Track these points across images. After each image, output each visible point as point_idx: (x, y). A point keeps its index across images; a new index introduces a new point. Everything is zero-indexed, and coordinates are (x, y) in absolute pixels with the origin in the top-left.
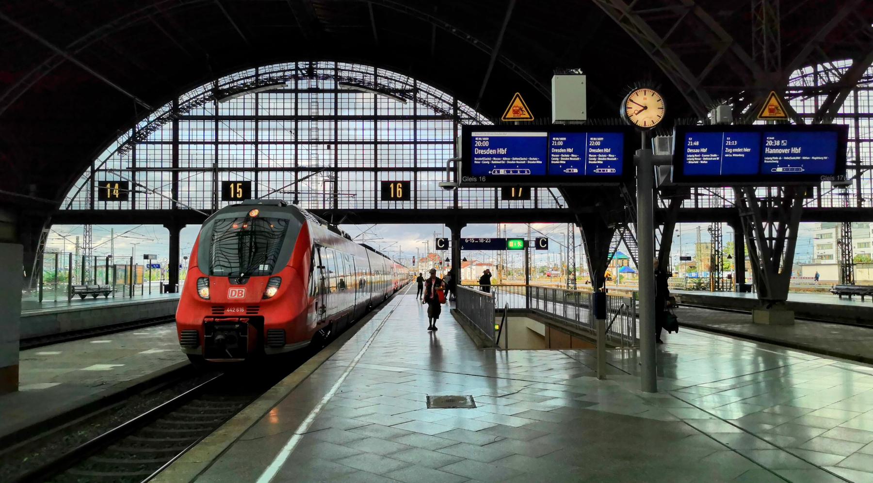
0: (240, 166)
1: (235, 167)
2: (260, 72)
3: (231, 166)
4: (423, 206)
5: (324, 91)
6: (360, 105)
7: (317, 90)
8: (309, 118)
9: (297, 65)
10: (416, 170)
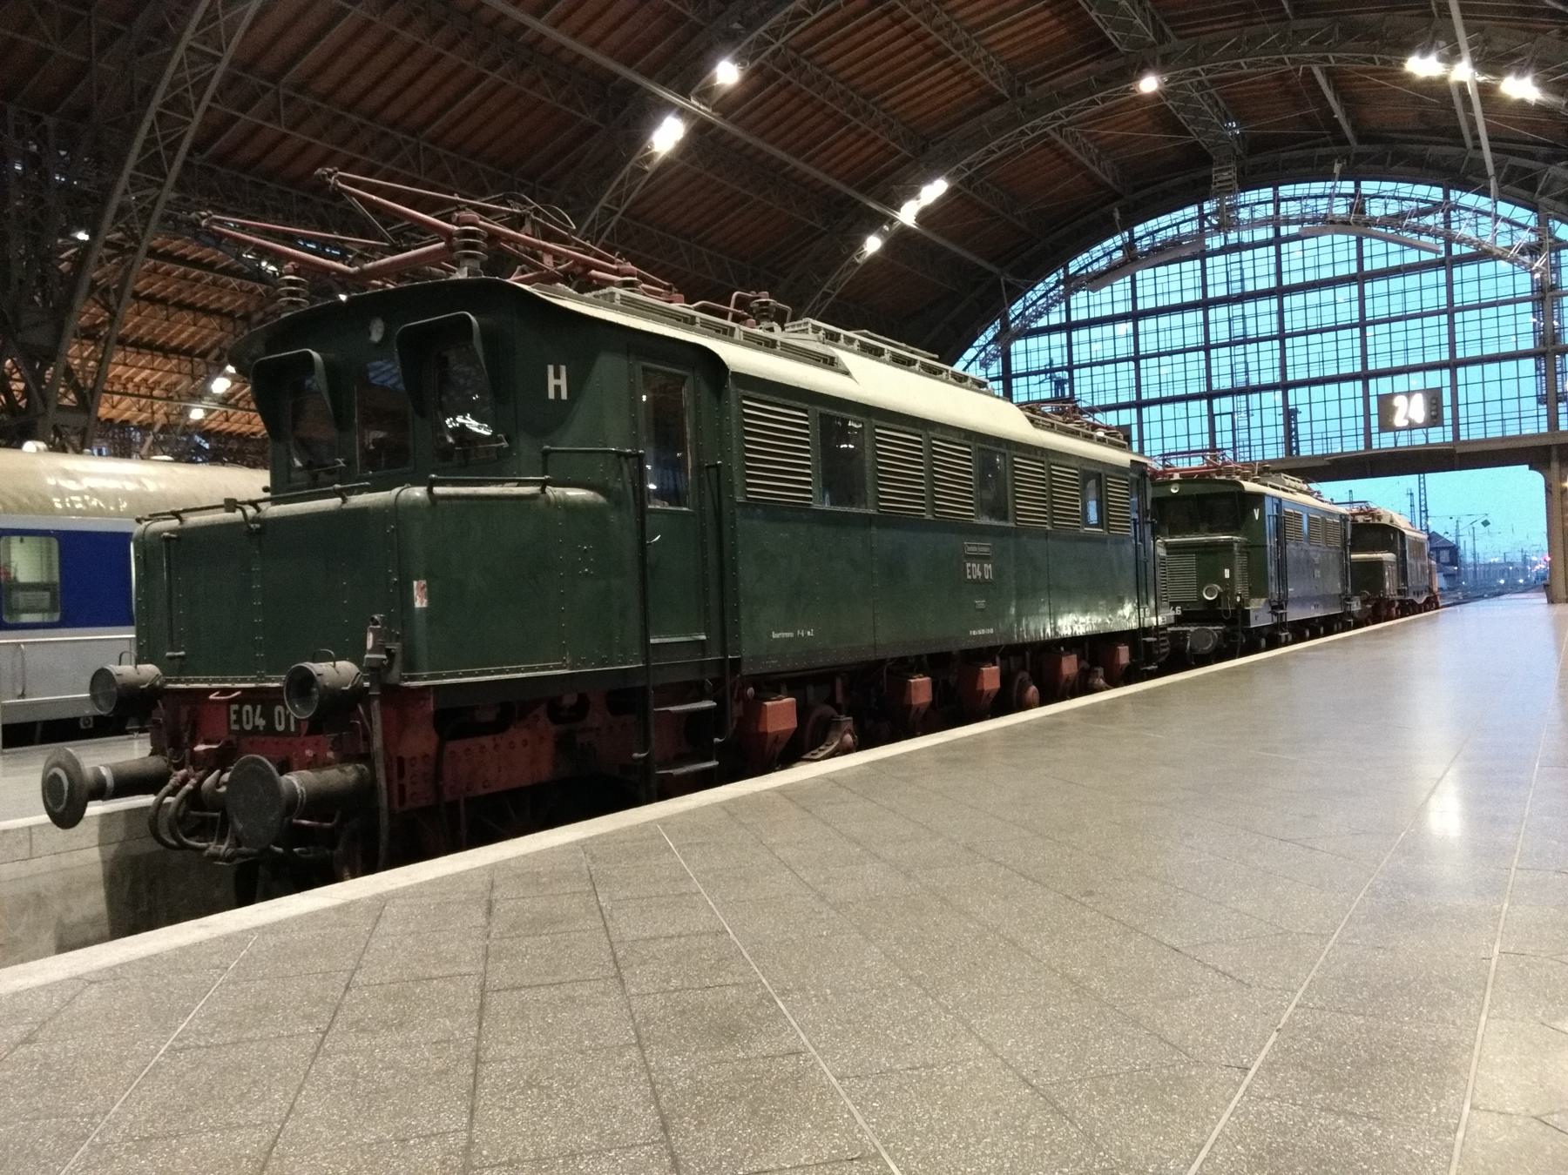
0: (1180, 392)
1: (1171, 394)
2: (1136, 235)
3: (1164, 395)
4: (1473, 432)
5: (1254, 245)
6: (1326, 259)
7: (1239, 247)
8: (1228, 300)
9: (1201, 209)
10: (1453, 365)
